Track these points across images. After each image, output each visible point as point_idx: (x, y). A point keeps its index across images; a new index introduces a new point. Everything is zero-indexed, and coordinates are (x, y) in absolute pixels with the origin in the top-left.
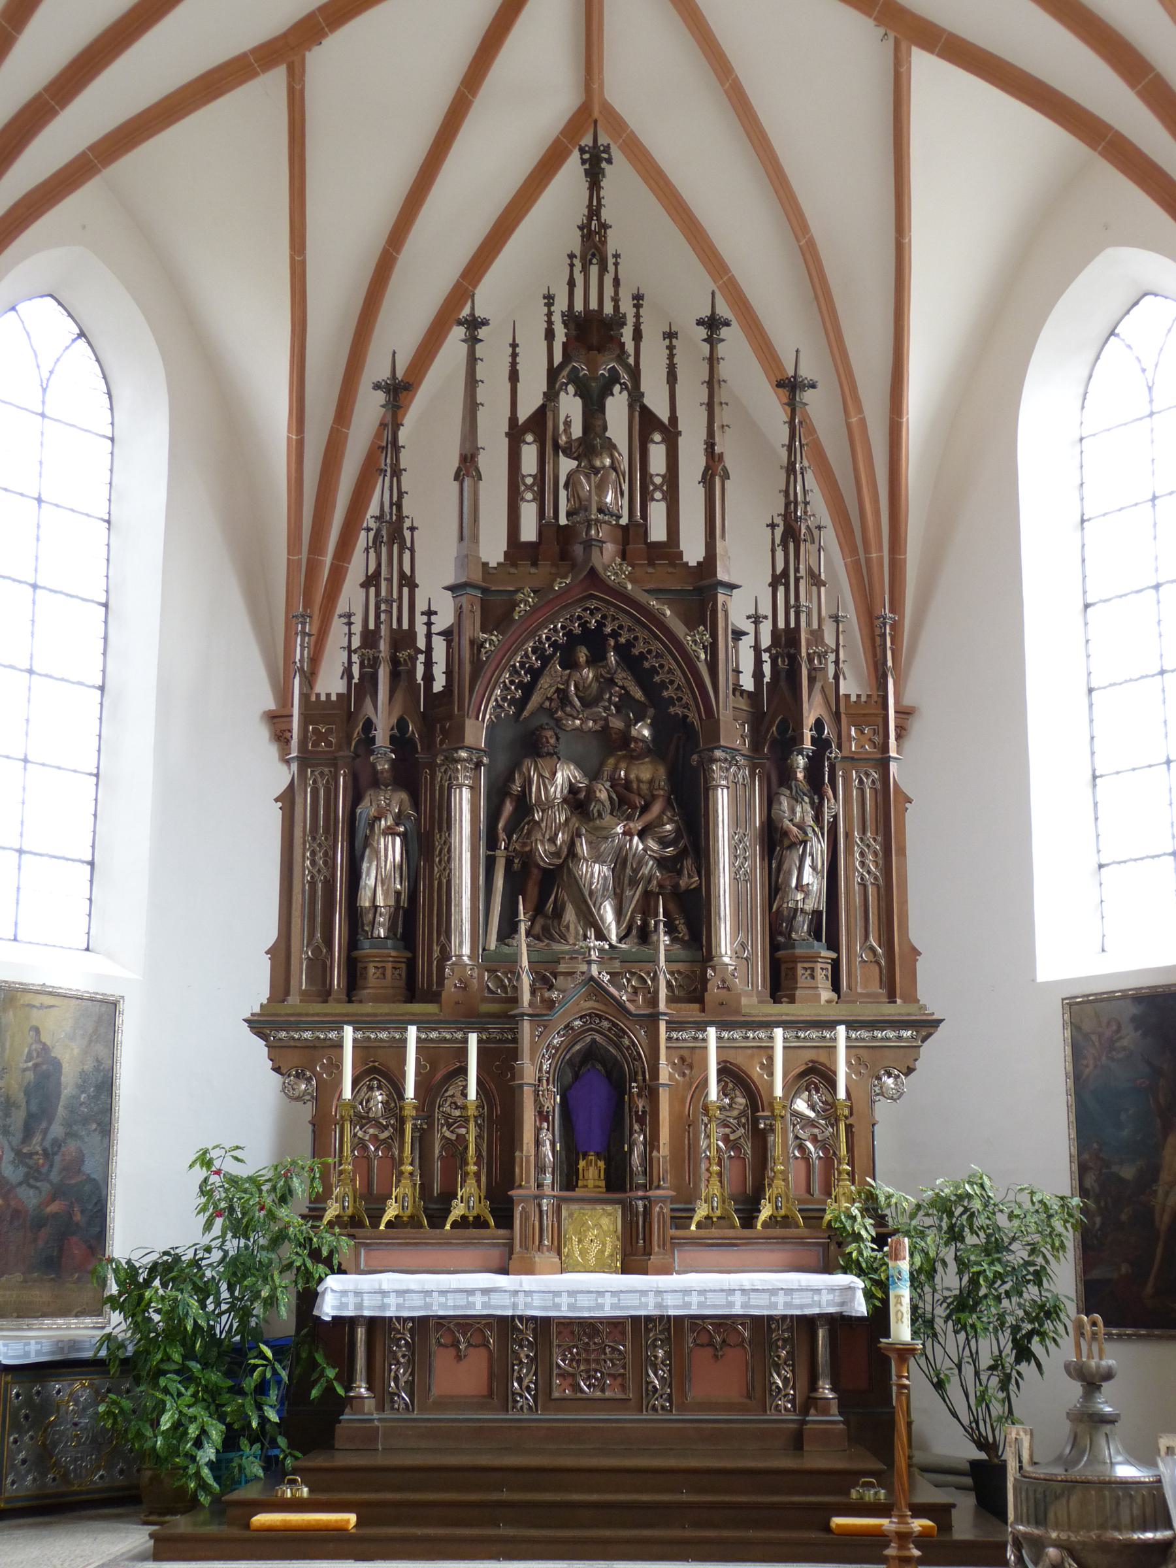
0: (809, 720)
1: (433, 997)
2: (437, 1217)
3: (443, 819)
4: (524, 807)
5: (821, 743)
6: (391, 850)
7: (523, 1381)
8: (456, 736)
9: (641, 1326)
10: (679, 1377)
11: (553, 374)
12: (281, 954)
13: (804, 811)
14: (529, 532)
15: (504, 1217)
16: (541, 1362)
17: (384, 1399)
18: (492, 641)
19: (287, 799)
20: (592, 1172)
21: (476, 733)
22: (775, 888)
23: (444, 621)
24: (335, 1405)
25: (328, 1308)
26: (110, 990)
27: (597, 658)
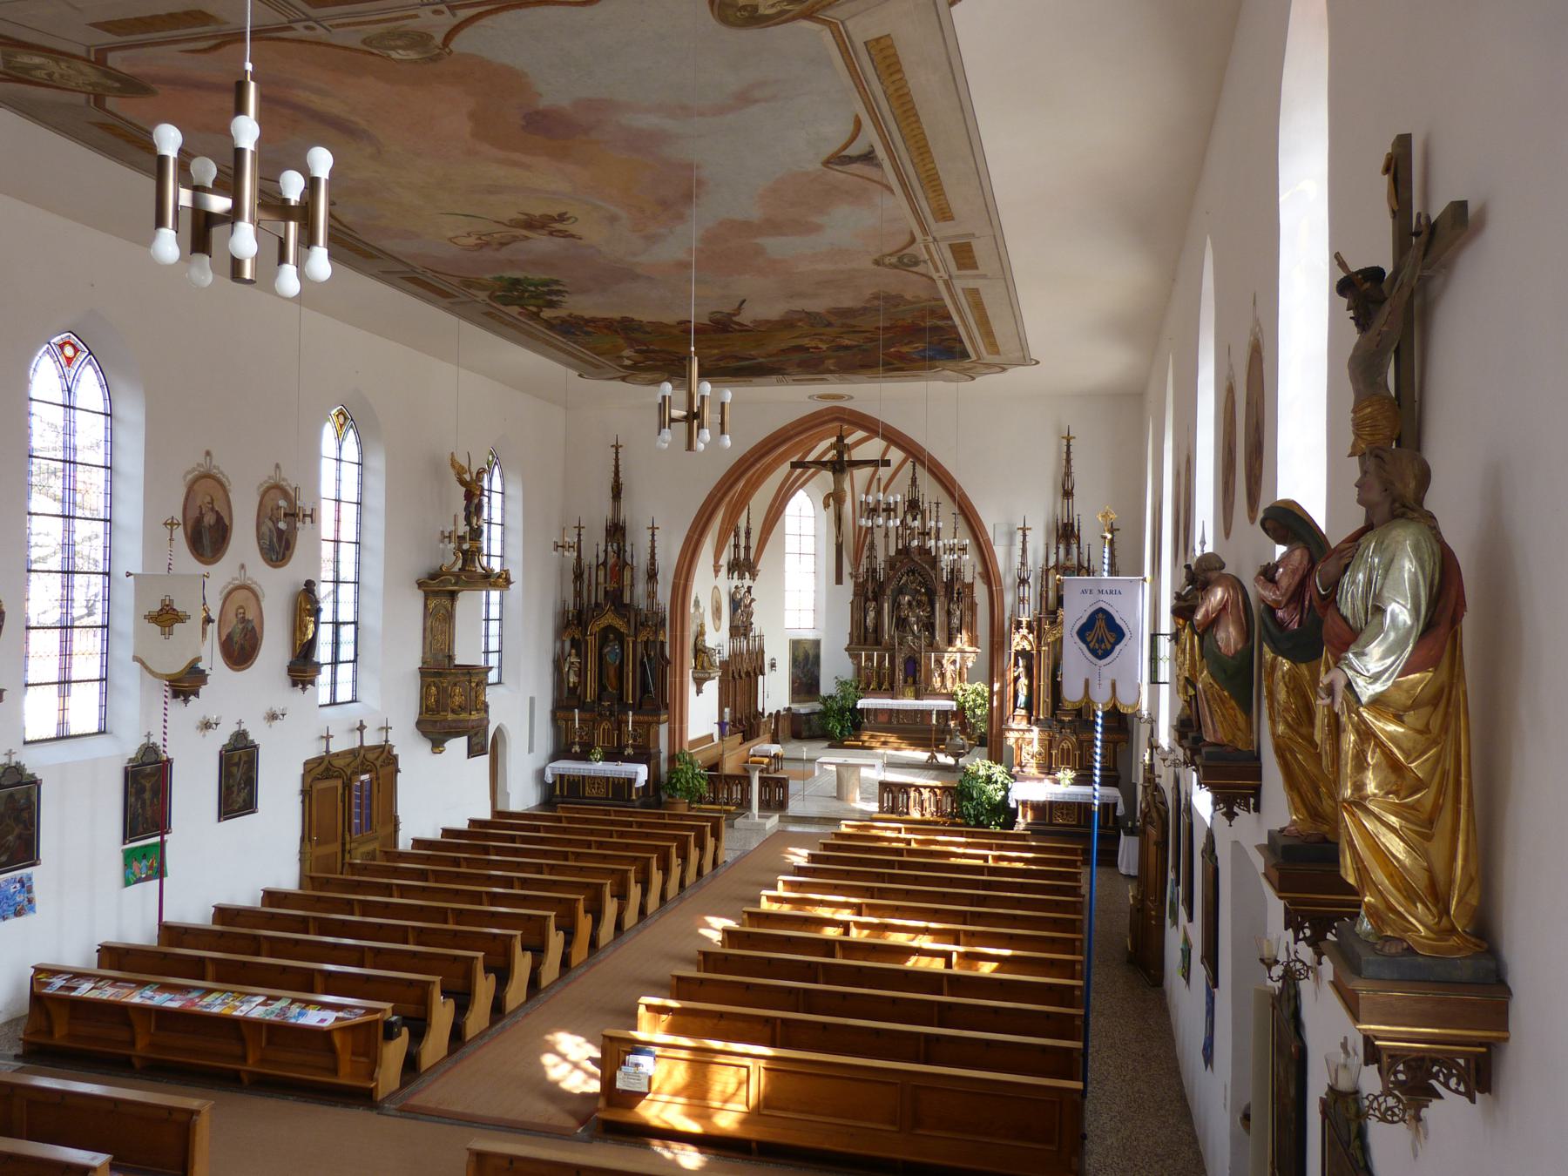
0: (956, 588)
1: (880, 644)
2: (880, 688)
3: (882, 608)
4: (899, 605)
5: (959, 593)
6: (872, 614)
7: (894, 721)
8: (884, 591)
9: (916, 712)
10: (922, 721)
11: (905, 512)
12: (851, 634)
13: (956, 606)
14: (900, 547)
15: (893, 689)
16: (898, 717)
17: (869, 722)
18: (891, 573)
19: (852, 603)
20: (910, 680)
21: (888, 592)
22: (949, 623)
23: (882, 566)
24: (860, 723)
25: (858, 707)
26: (818, 638)
27: (914, 574)
